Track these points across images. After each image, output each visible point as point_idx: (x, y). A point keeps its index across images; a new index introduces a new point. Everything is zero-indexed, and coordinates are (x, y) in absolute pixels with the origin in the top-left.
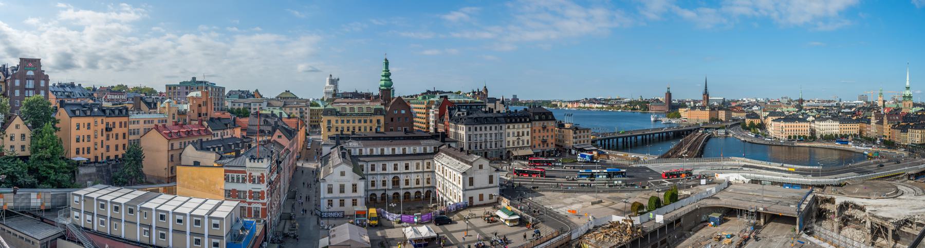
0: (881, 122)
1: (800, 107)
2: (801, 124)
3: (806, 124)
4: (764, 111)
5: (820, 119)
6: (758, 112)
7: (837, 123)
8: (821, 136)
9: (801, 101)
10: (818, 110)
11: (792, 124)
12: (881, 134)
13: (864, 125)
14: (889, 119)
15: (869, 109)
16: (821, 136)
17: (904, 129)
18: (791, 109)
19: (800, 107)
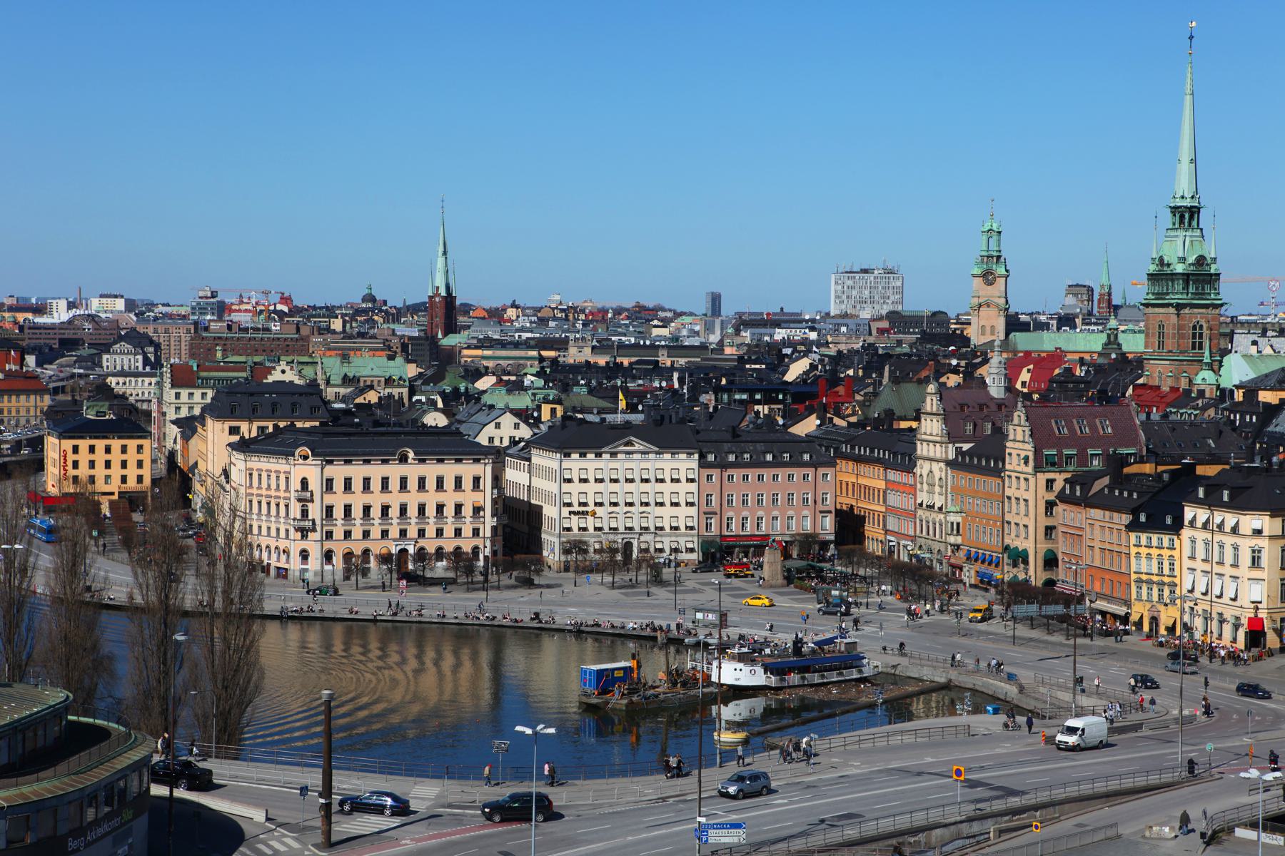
0: (982, 457)
1: (436, 360)
2: (431, 470)
3: (468, 470)
4: (182, 378)
5: (572, 437)
6: (139, 389)
7: (686, 464)
8: (575, 547)
9: (449, 311)
10: (560, 376)
11: (376, 471)
12: (988, 541)
13: (874, 478)
14: (1039, 436)
15: (909, 369)
16: (575, 547)
17: (1158, 511)
18: (370, 365)
19: (436, 360)
